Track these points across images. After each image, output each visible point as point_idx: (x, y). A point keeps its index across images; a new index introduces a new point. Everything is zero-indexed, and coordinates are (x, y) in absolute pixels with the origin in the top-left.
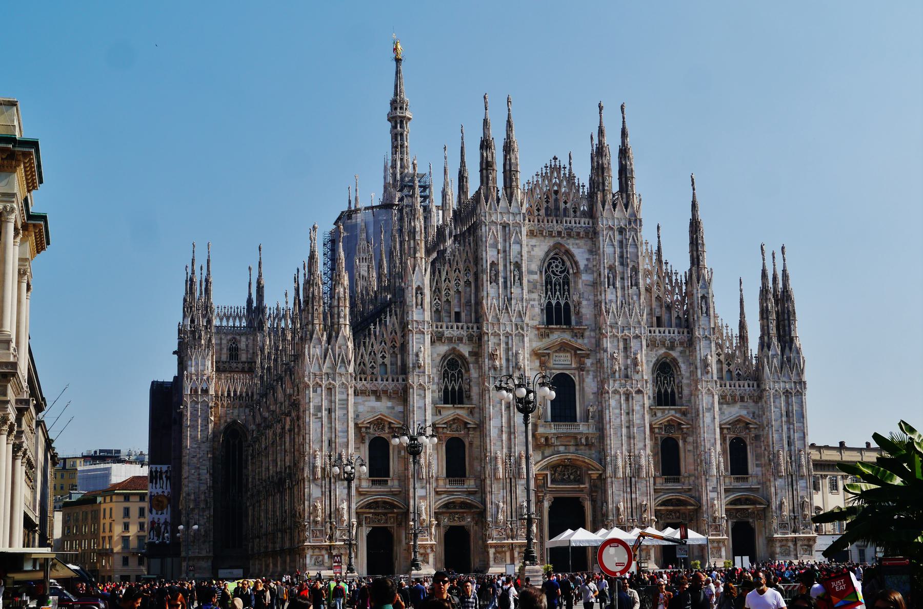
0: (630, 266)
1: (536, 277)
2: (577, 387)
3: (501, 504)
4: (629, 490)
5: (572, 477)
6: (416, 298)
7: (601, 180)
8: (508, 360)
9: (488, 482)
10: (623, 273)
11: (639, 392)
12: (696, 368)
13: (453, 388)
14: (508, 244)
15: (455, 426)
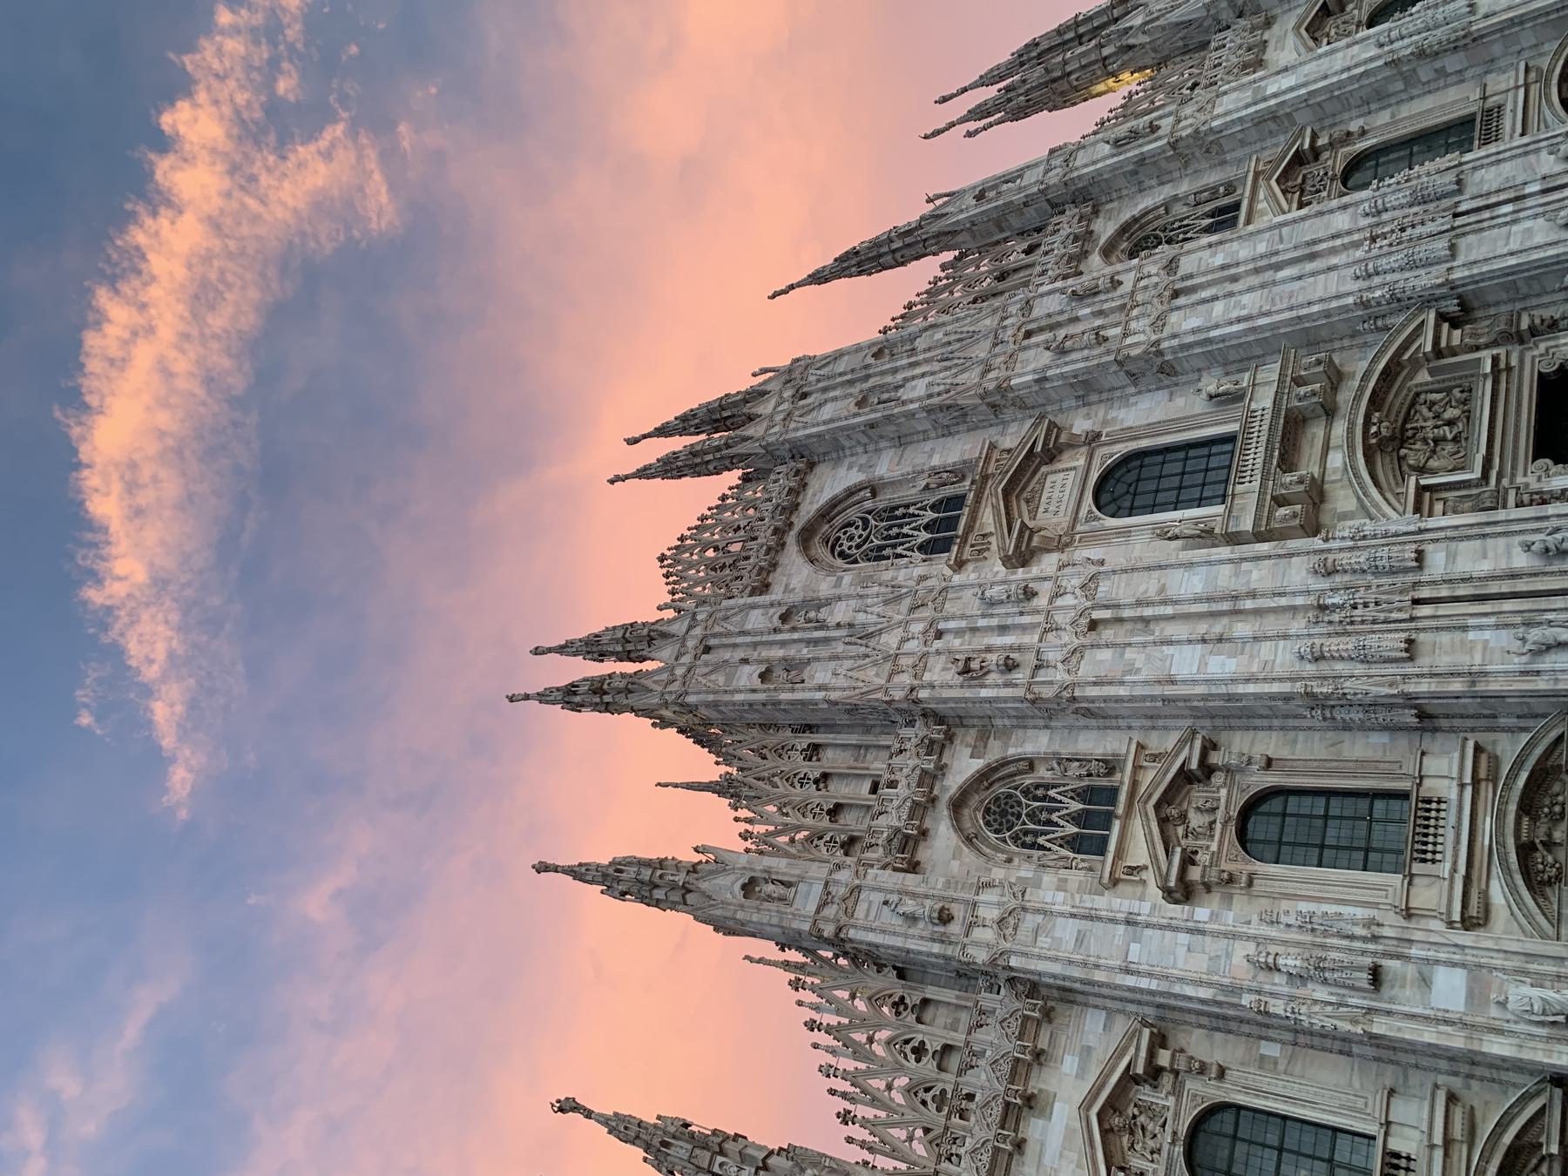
0: (872, 361)
1: (847, 578)
2: (1144, 443)
3: (1535, 634)
4: (1508, 208)
5: (1450, 413)
6: (769, 898)
7: (710, 457)
8: (1003, 629)
9: (1424, 687)
10: (883, 373)
11: (1171, 266)
12: (1142, 160)
13: (1075, 819)
14: (739, 640)
15: (1196, 820)
